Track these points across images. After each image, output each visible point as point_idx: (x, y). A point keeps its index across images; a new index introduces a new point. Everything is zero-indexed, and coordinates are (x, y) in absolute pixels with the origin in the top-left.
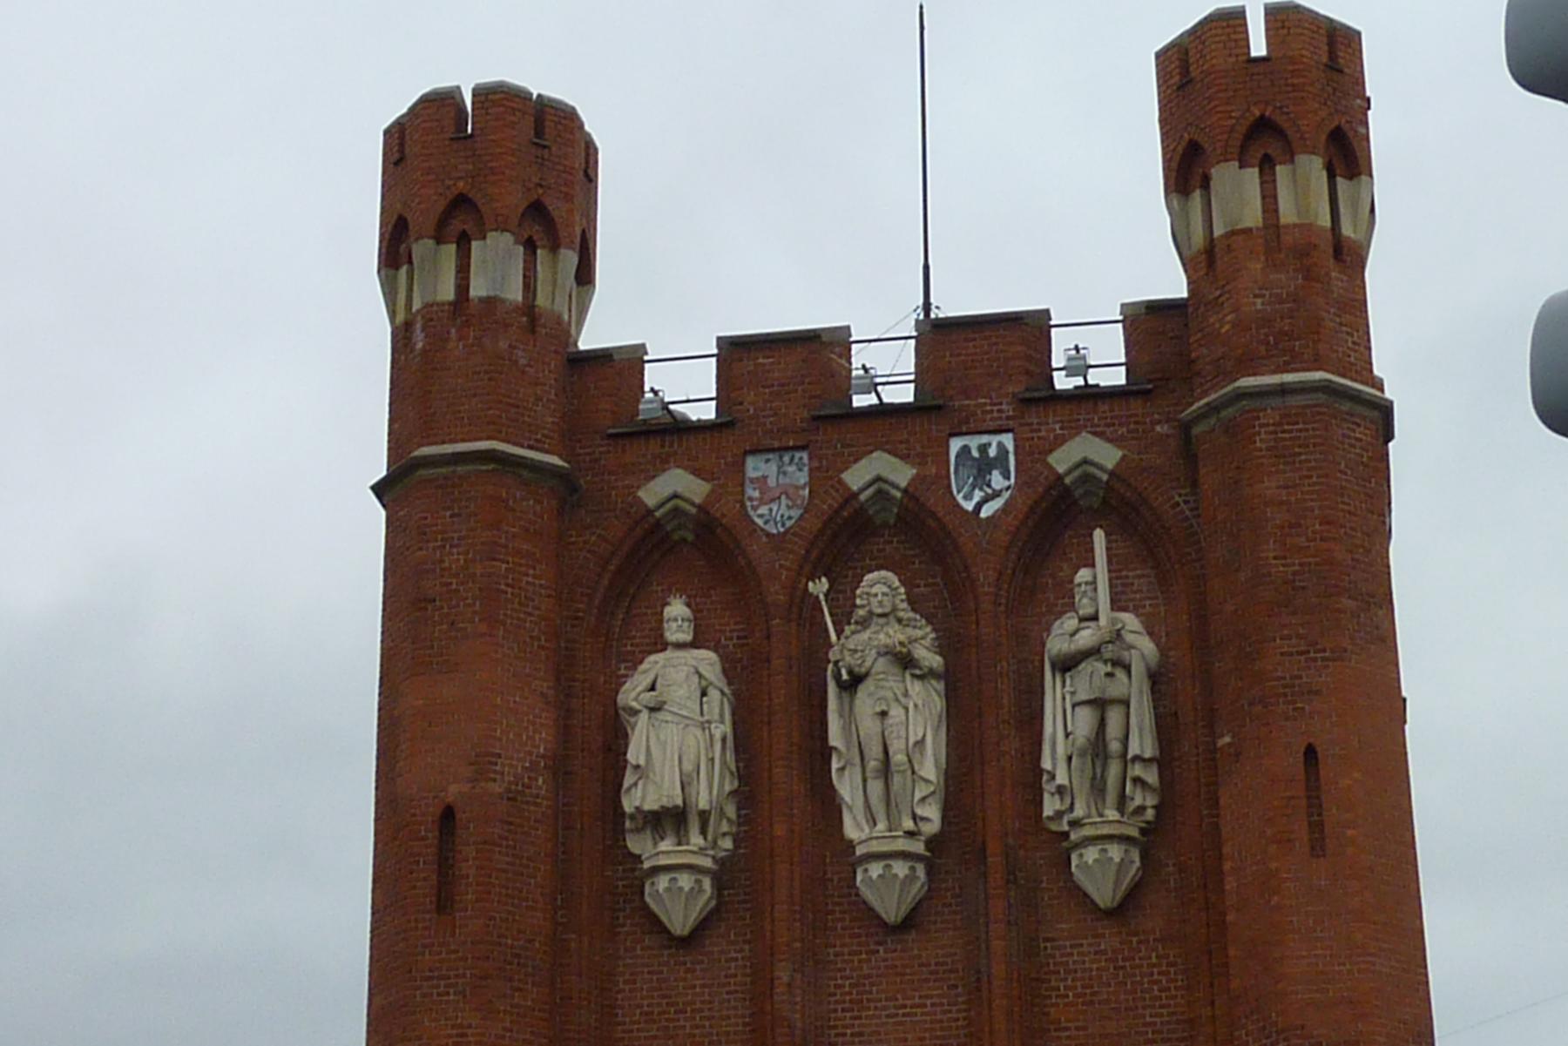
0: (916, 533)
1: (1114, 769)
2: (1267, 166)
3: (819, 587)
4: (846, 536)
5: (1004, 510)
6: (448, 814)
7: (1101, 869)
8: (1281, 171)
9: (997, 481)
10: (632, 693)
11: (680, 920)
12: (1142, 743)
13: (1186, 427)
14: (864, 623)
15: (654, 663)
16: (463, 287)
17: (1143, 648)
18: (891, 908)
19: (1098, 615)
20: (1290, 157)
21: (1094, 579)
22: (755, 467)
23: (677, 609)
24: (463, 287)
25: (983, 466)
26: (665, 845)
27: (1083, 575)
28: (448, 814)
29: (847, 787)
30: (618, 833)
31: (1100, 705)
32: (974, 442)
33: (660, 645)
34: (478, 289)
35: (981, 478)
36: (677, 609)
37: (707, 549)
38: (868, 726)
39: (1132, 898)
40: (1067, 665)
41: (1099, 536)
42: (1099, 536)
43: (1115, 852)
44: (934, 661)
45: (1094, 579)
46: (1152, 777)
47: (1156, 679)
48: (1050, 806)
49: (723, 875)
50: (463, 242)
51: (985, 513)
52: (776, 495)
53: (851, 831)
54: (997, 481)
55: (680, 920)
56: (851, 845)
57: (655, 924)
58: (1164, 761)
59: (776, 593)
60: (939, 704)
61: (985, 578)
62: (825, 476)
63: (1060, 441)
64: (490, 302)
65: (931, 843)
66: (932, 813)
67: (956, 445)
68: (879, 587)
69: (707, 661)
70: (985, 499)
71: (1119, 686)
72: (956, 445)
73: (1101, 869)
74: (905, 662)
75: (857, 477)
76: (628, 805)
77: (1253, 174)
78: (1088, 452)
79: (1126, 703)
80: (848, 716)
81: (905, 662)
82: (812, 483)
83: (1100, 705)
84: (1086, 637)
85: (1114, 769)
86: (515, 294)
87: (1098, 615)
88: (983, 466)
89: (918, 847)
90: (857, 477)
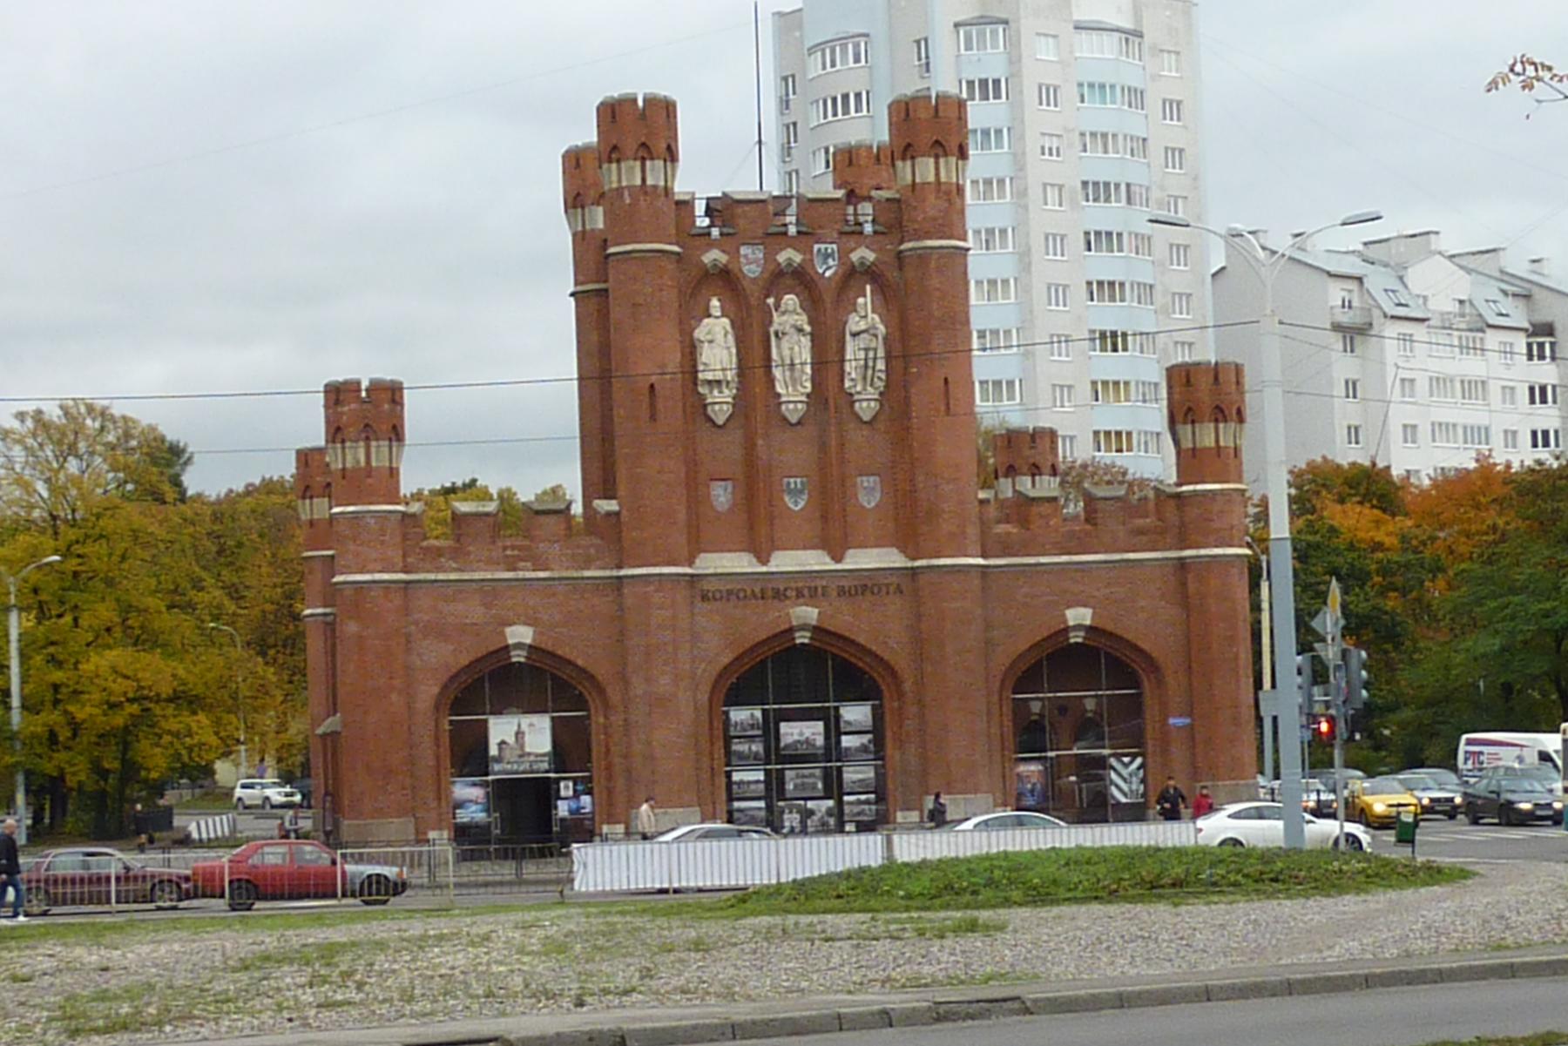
0: (801, 279)
1: (870, 372)
2: (937, 157)
3: (771, 301)
4: (778, 280)
5: (835, 273)
6: (652, 386)
7: (867, 407)
8: (942, 161)
9: (831, 262)
10: (699, 333)
11: (720, 421)
12: (881, 365)
13: (901, 252)
14: (784, 313)
15: (706, 321)
16: (644, 180)
17: (882, 329)
18: (794, 419)
19: (865, 317)
20: (946, 155)
21: (865, 301)
22: (743, 250)
23: (715, 303)
24: (644, 180)
25: (827, 256)
26: (716, 392)
27: (861, 300)
28: (652, 386)
29: (777, 373)
30: (696, 384)
31: (867, 350)
32: (823, 246)
33: (709, 316)
34: (649, 182)
35: (825, 262)
36: (715, 303)
37: (726, 279)
38: (786, 353)
39: (875, 417)
40: (854, 335)
41: (868, 288)
42: (868, 288)
43: (873, 404)
44: (808, 328)
45: (865, 301)
46: (883, 376)
47: (885, 339)
48: (847, 384)
49: (738, 401)
50: (643, 159)
51: (828, 274)
52: (751, 261)
53: (779, 389)
54: (831, 262)
55: (720, 421)
56: (779, 395)
57: (710, 420)
58: (887, 371)
59: (753, 301)
60: (809, 344)
61: (828, 298)
62: (769, 256)
63: (853, 250)
64: (655, 187)
65: (808, 396)
66: (808, 384)
67: (816, 247)
68: (790, 300)
69: (726, 321)
70: (828, 270)
71: (873, 345)
72: (816, 247)
73: (867, 407)
74: (800, 330)
75: (782, 258)
76: (701, 376)
77: (932, 160)
78: (863, 254)
79: (875, 350)
80: (778, 347)
81: (800, 330)
82: (765, 258)
83: (867, 350)
84: (862, 325)
85: (870, 372)
86: (662, 183)
87: (865, 317)
88: (827, 256)
89: (804, 398)
90: (782, 258)
